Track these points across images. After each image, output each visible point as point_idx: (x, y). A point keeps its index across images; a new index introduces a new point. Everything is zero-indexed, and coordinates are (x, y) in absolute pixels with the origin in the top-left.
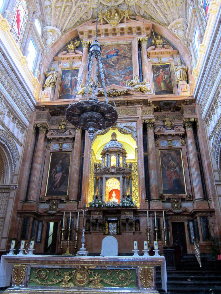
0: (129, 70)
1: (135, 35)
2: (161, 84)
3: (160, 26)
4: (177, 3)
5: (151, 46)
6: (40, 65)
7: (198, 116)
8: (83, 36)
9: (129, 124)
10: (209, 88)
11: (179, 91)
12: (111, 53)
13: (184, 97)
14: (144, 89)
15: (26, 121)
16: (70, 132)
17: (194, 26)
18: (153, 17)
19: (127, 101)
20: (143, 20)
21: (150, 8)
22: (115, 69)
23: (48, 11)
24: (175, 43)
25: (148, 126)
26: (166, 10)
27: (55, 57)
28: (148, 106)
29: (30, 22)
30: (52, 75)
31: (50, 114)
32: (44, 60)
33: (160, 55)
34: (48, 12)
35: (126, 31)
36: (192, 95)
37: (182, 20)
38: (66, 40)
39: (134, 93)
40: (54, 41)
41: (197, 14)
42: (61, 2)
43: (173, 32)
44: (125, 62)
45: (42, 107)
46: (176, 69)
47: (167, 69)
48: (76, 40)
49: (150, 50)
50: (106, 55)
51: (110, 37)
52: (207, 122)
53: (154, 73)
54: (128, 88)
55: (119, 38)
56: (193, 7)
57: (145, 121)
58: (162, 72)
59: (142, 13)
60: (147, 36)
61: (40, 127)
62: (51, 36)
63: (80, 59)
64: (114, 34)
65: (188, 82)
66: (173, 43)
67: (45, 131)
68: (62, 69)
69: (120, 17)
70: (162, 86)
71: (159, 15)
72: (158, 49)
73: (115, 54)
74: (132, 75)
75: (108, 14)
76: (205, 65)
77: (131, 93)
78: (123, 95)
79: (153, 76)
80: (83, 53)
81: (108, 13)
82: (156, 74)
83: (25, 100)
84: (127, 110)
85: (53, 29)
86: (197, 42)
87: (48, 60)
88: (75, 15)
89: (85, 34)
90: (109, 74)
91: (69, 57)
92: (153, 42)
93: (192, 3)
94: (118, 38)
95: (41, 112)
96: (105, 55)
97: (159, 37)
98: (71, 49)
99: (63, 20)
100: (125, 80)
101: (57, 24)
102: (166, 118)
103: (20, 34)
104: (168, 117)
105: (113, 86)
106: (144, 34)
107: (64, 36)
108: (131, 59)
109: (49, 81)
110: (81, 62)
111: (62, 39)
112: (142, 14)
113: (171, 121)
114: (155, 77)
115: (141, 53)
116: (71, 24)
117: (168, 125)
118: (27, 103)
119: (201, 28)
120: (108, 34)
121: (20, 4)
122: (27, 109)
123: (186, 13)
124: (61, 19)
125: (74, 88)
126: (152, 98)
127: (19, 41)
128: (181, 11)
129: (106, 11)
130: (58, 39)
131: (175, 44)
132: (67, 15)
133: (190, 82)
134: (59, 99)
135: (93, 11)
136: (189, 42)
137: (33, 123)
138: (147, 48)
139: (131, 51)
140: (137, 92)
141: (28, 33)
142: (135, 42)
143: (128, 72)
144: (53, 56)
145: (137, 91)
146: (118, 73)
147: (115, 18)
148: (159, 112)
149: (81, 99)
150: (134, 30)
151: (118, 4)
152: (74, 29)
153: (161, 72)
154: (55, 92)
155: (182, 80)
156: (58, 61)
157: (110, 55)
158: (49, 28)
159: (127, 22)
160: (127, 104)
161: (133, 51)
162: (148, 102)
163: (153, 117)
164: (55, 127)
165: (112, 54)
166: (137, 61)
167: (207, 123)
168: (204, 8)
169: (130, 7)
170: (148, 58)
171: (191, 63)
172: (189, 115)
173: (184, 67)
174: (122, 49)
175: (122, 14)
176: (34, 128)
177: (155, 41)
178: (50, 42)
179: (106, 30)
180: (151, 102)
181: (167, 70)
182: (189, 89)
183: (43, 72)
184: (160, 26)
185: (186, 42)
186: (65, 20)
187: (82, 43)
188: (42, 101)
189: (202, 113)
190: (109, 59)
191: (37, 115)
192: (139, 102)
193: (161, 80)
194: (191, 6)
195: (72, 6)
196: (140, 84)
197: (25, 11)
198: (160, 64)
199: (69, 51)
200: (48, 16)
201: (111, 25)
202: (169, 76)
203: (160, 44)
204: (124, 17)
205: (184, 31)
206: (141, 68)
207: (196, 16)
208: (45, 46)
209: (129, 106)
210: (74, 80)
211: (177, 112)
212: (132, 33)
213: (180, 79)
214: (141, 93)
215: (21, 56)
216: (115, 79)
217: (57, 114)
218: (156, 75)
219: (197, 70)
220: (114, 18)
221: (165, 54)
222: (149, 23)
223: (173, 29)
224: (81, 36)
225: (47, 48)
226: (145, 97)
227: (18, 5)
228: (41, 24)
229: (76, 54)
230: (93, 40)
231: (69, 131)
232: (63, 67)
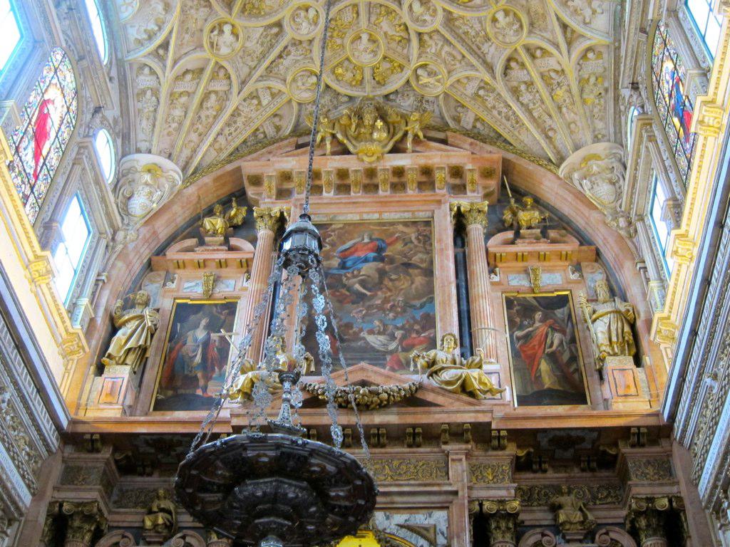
0: (422, 312)
1: (444, 191)
2: (539, 364)
3: (531, 167)
4: (585, 96)
5: (500, 231)
6: (96, 285)
7: (683, 489)
9: (420, 519)
10: (716, 386)
11: (607, 395)
12: (356, 250)
13: (626, 416)
14: (476, 385)
15: (19, 490)
16: (188, 539)
17: (649, 169)
19: (414, 426)
20: (471, 144)
21: (494, 107)
22: (369, 308)
23: (145, 106)
24: (586, 223)
25: (493, 526)
26: (550, 116)
27: (155, 258)
28: (495, 449)
29: (79, 139)
30: (137, 323)
31: (114, 467)
32: (113, 265)
34: (146, 110)
35: (413, 177)
36: (656, 408)
37: (605, 149)
38: (198, 203)
39: (440, 399)
40: (155, 205)
41: (656, 133)
42: (193, 79)
43: (575, 188)
44: (406, 285)
45: (88, 437)
46: (594, 312)
47: (560, 313)
48: (234, 204)
49: (496, 246)
50: (340, 258)
52: (717, 513)
53: (512, 324)
54: (417, 378)
55: (386, 202)
56: (639, 109)
57: (481, 505)
58: (540, 321)
59: (468, 121)
60: (486, 196)
61: (72, 515)
62: (147, 184)
63: (245, 270)
64: (371, 188)
65: (638, 361)
66: (580, 222)
67: (89, 531)
68: (175, 299)
69: (391, 134)
70: (543, 375)
71: (527, 129)
72: (527, 241)
73: (372, 255)
74: (432, 331)
75: (351, 124)
76: (697, 303)
77: (430, 397)
78: (396, 404)
79: (511, 336)
82: (521, 327)
83: (27, 408)
84: (413, 461)
85: (155, 164)
86: (663, 224)
87: (128, 266)
88: (235, 122)
89: (266, 184)
90: (349, 326)
91: (205, 261)
92: (508, 216)
93: (635, 97)
94: (381, 202)
95: (83, 455)
96: (335, 256)
97: (529, 201)
98: (215, 234)
99: (194, 137)
100: (407, 349)
101: (173, 147)
102: (562, 494)
103: (40, 177)
104: (569, 493)
105: (362, 369)
106: (474, 191)
107: (192, 190)
108: (429, 272)
109: (124, 341)
111: (185, 199)
112: (469, 127)
113: (581, 509)
114: (519, 339)
115: (464, 253)
116: (221, 149)
117: (571, 523)
118: (34, 420)
119: (672, 176)
120: (350, 186)
121: (55, 81)
122: (31, 444)
123: (618, 128)
124: (188, 132)
125: (213, 370)
126: (506, 418)
127: (32, 200)
128: (601, 120)
129: (346, 111)
130: (172, 197)
131: (586, 226)
132: (211, 120)
133: (647, 360)
134: (155, 409)
135: (300, 111)
136: (634, 221)
137: (48, 499)
138: (488, 236)
139: (431, 245)
140: (451, 395)
141: (67, 175)
142: (445, 216)
143: (416, 322)
144: (146, 253)
145: (450, 391)
146: (381, 321)
147: (376, 135)
148: (535, 472)
149: (238, 416)
150: (438, 175)
151: (386, 92)
152: (229, 167)
153: (537, 324)
154: (141, 382)
155: (615, 354)
156: (163, 273)
157: (351, 258)
158: (143, 160)
159: (418, 149)
160: (414, 439)
161: (436, 245)
162: (494, 433)
163: (513, 492)
164: (130, 517)
165: (362, 254)
166: (450, 283)
167: (718, 518)
168: (677, 115)
169: (427, 101)
170: (492, 271)
171: (644, 295)
172: (650, 485)
173: (622, 307)
174: (397, 239)
175: (399, 123)
176: (47, 519)
178: (140, 204)
179: (343, 174)
180: (503, 433)
181: (559, 315)
182: (643, 385)
183: (106, 310)
184: (531, 167)
186: (202, 136)
187: (255, 214)
188: (91, 414)
189: (700, 477)
190: (350, 271)
191: (67, 468)
192: (457, 433)
193: (541, 351)
194: (633, 108)
195: (227, 93)
196: (461, 364)
197: (68, 104)
199: (207, 239)
200: (144, 122)
201: (358, 159)
202: (568, 337)
203: (533, 225)
204: (406, 134)
205: (614, 184)
206: (464, 307)
207: (652, 138)
208: (123, 219)
209: (419, 446)
210: (217, 344)
211: (604, 473)
212: (434, 185)
213: (608, 349)
214: (465, 397)
215: (34, 252)
216: (367, 343)
217: (144, 467)
218: (519, 333)
219: (668, 318)
220: (371, 134)
221: (549, 260)
222: (494, 155)
223: (576, 176)
224: (251, 192)
225: (128, 224)
226: (479, 415)
227: (48, 87)
228: (115, 146)
229: (232, 249)
230: (296, 206)
231: (183, 537)
232: (181, 294)
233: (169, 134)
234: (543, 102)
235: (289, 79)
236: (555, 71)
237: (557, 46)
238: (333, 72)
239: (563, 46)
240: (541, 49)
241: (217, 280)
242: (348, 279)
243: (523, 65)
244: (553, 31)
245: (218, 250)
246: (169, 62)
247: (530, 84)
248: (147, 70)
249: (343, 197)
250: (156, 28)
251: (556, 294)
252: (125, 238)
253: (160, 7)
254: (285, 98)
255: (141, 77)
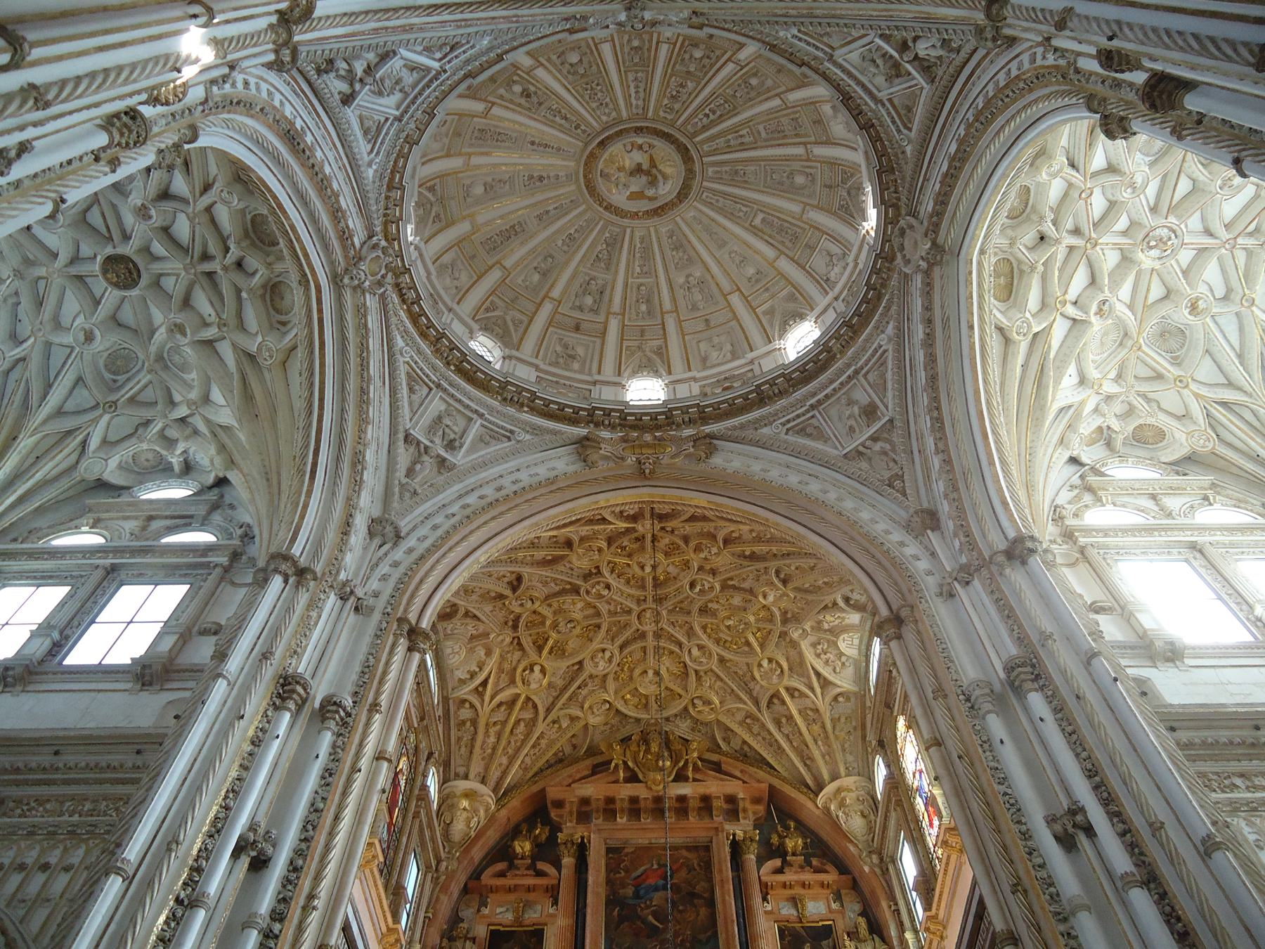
6: (424, 922)
8: (560, 811)
12: (647, 877)
18: (771, 761)
20: (742, 771)
21: (759, 734)
33: (798, 891)
35: (693, 804)
48: (539, 825)
51: (645, 824)
59: (736, 744)
62: (464, 809)
66: (837, 850)
69: (675, 763)
72: (793, 869)
80: (559, 870)
81: (639, 746)
91: (515, 886)
92: (775, 840)
96: (629, 884)
97: (792, 824)
99: (505, 761)
101: (487, 769)
107: (503, 812)
108: (711, 903)
110: (555, 903)
112: (738, 748)
138: (761, 861)
144: (462, 878)
150: (716, 803)
156: (477, 898)
158: (462, 785)
165: (651, 881)
169: (702, 723)
170: (765, 899)
175: (680, 750)
177: (780, 837)
179: (634, 800)
185: (875, 858)
195: (534, 720)
198: (801, 922)
199: (516, 862)
200: (463, 749)
201: (647, 786)
204: (687, 761)
229: (540, 874)
233: (483, 759)
234: (801, 734)
235: (586, 706)
236: (811, 709)
237: (812, 689)
238: (623, 697)
239: (818, 691)
240: (799, 691)
241: (528, 905)
242: (642, 909)
243: (783, 702)
244: (809, 678)
245: (527, 875)
246: (487, 698)
247: (790, 718)
248: (467, 705)
249: (635, 824)
250: (477, 670)
251: (820, 924)
252: (447, 868)
253: (482, 653)
254: (582, 723)
255: (462, 710)
